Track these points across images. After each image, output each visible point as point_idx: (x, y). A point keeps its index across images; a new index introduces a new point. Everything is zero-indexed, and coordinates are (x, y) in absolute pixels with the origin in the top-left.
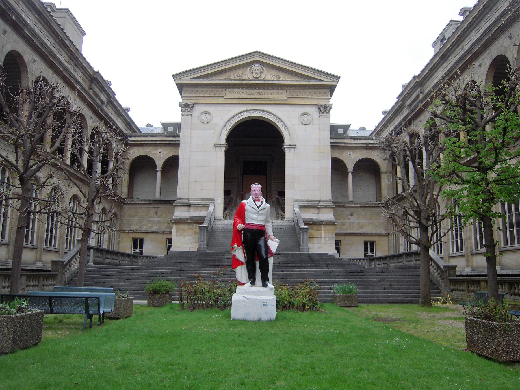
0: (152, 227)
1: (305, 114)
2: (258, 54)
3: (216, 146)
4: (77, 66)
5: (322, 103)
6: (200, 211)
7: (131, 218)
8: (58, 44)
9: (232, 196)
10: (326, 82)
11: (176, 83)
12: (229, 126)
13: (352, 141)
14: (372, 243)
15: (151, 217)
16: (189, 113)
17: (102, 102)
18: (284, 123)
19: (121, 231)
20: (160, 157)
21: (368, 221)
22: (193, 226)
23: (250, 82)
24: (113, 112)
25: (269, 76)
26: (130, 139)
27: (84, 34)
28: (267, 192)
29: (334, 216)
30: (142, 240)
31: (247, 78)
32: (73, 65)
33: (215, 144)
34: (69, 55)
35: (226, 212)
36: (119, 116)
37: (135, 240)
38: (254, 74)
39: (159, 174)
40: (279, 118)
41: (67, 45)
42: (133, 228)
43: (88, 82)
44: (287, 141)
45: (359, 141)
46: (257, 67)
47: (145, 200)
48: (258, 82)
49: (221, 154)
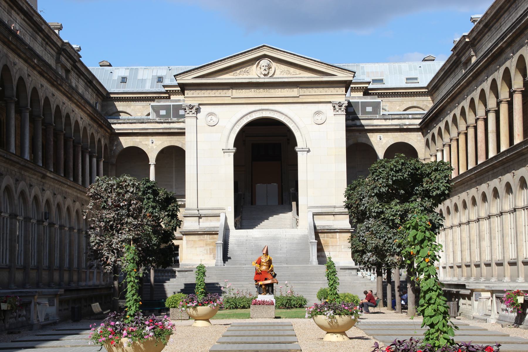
1: (318, 113)
3: (225, 151)
6: (211, 221)
18: (295, 124)
20: (152, 147)
28: (282, 183)
29: (351, 222)
35: (237, 219)
36: (80, 77)
39: (152, 169)
40: (290, 118)
44: (300, 144)
46: (264, 62)
49: (230, 159)
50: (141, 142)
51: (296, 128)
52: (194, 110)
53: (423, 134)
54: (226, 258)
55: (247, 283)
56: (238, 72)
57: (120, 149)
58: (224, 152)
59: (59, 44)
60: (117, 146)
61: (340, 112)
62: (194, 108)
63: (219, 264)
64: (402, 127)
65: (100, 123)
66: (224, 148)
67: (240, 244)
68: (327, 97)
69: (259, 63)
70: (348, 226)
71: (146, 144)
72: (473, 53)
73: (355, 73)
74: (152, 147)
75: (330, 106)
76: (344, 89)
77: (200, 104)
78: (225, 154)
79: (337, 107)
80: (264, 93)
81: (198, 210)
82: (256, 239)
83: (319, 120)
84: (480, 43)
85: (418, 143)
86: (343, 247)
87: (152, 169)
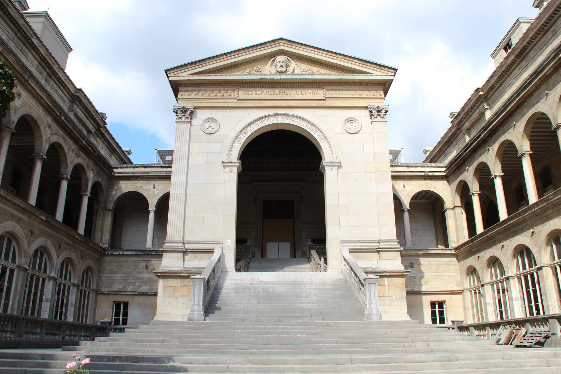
0: (141, 287)
1: (350, 120)
2: (283, 41)
4: (51, 77)
5: (374, 104)
6: (201, 259)
7: (113, 275)
8: (21, 41)
9: (248, 244)
10: (378, 75)
11: (170, 81)
12: (244, 138)
13: (406, 169)
14: (441, 304)
15: (140, 273)
16: (187, 120)
17: (89, 132)
18: (321, 132)
19: (98, 292)
21: (434, 274)
22: (189, 282)
23: (272, 77)
24: (105, 147)
25: (299, 70)
26: (115, 170)
27: (70, 49)
28: (294, 241)
30: (126, 305)
31: (268, 73)
32: (45, 74)
33: (223, 162)
34: (39, 59)
36: (112, 154)
37: (118, 305)
38: (278, 68)
39: (152, 215)
40: (314, 125)
41: (33, 43)
42: (115, 288)
43: (68, 102)
44: (327, 156)
45: (413, 169)
46: (281, 58)
47: (132, 250)
48: (283, 77)
50: (142, 187)
51: (323, 137)
52: (187, 114)
53: (448, 182)
54: (210, 306)
55: (241, 358)
56: (248, 71)
57: (119, 194)
58: (224, 166)
59: (72, 90)
60: (116, 190)
61: (379, 119)
62: (189, 112)
63: (196, 317)
64: (427, 174)
65: (81, 143)
66: (224, 161)
67: (240, 289)
68: (361, 100)
69: (274, 60)
70: (401, 268)
71: (147, 189)
72: (486, 107)
73: (396, 70)
74: (154, 193)
75: (367, 112)
76: (382, 93)
77: (195, 108)
78: (226, 168)
79: (375, 112)
80: (280, 95)
81: (184, 243)
82: (267, 283)
83: (352, 128)
84: (503, 86)
85: (445, 191)
86: (394, 299)
87: (152, 215)
